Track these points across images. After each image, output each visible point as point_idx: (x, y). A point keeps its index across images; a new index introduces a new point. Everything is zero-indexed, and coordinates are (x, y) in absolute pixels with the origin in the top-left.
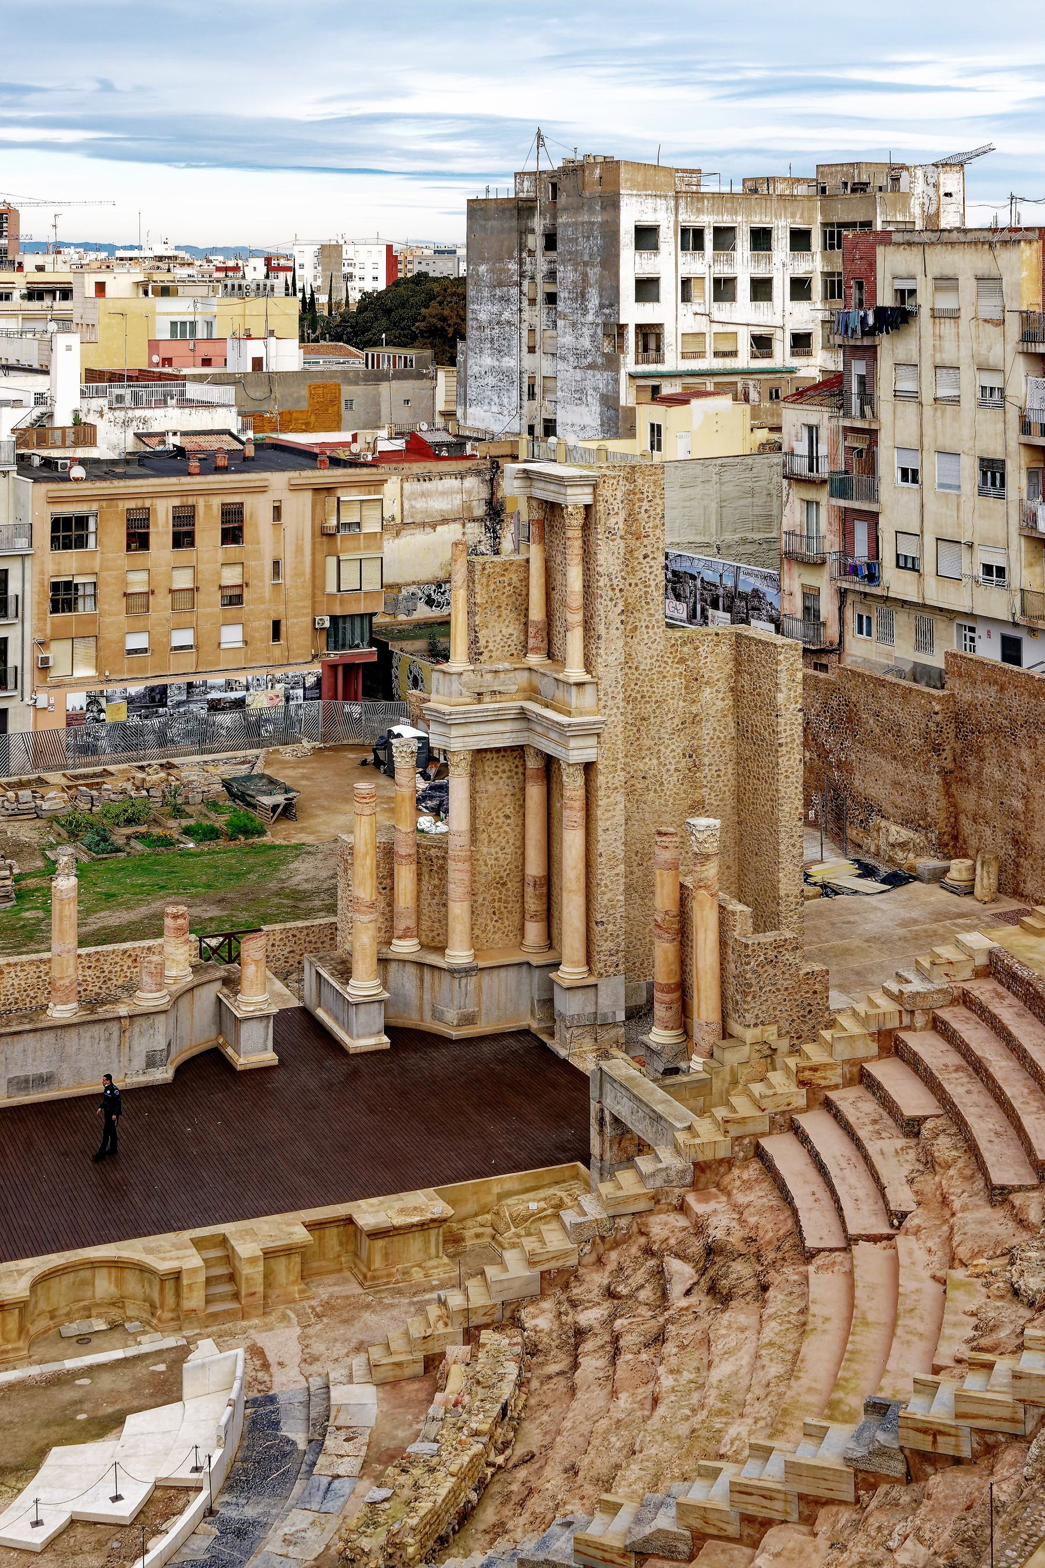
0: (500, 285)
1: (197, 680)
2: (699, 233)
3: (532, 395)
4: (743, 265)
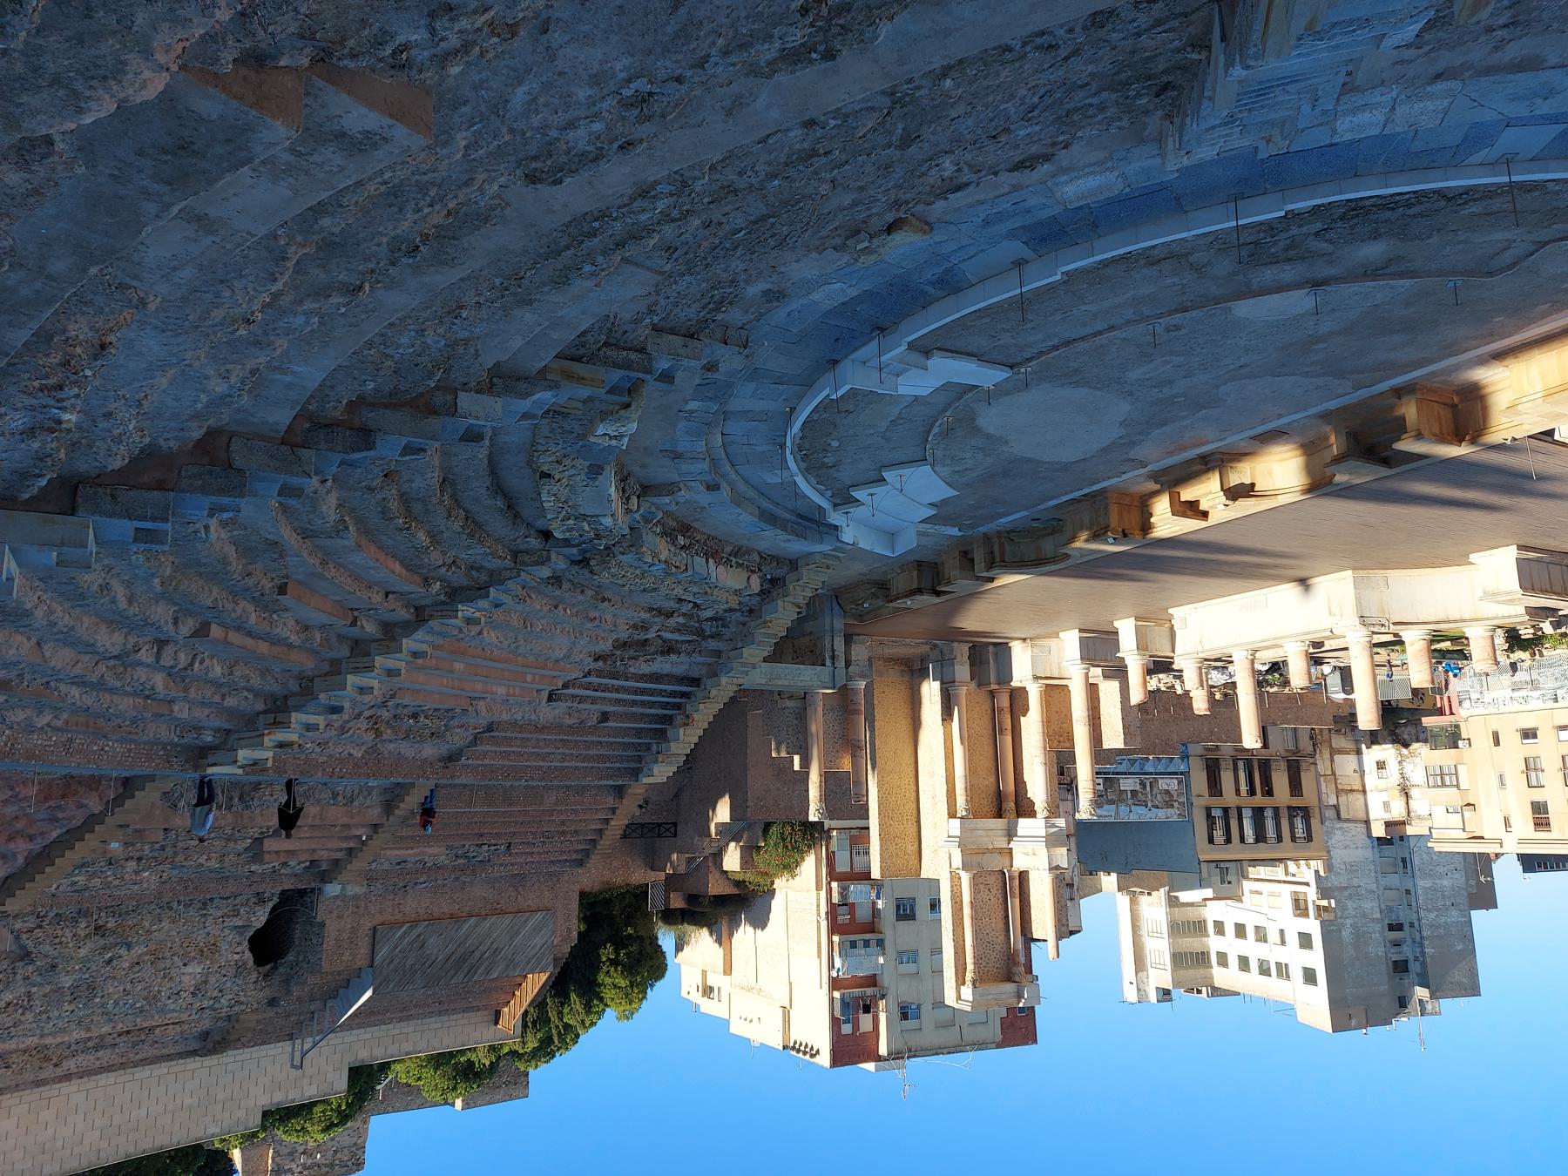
1: (1551, 704)
3: (1404, 860)
4: (1251, 948)
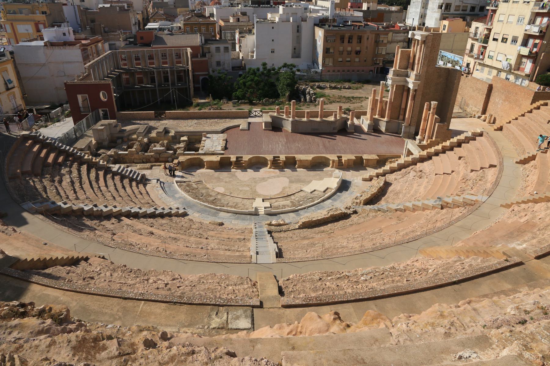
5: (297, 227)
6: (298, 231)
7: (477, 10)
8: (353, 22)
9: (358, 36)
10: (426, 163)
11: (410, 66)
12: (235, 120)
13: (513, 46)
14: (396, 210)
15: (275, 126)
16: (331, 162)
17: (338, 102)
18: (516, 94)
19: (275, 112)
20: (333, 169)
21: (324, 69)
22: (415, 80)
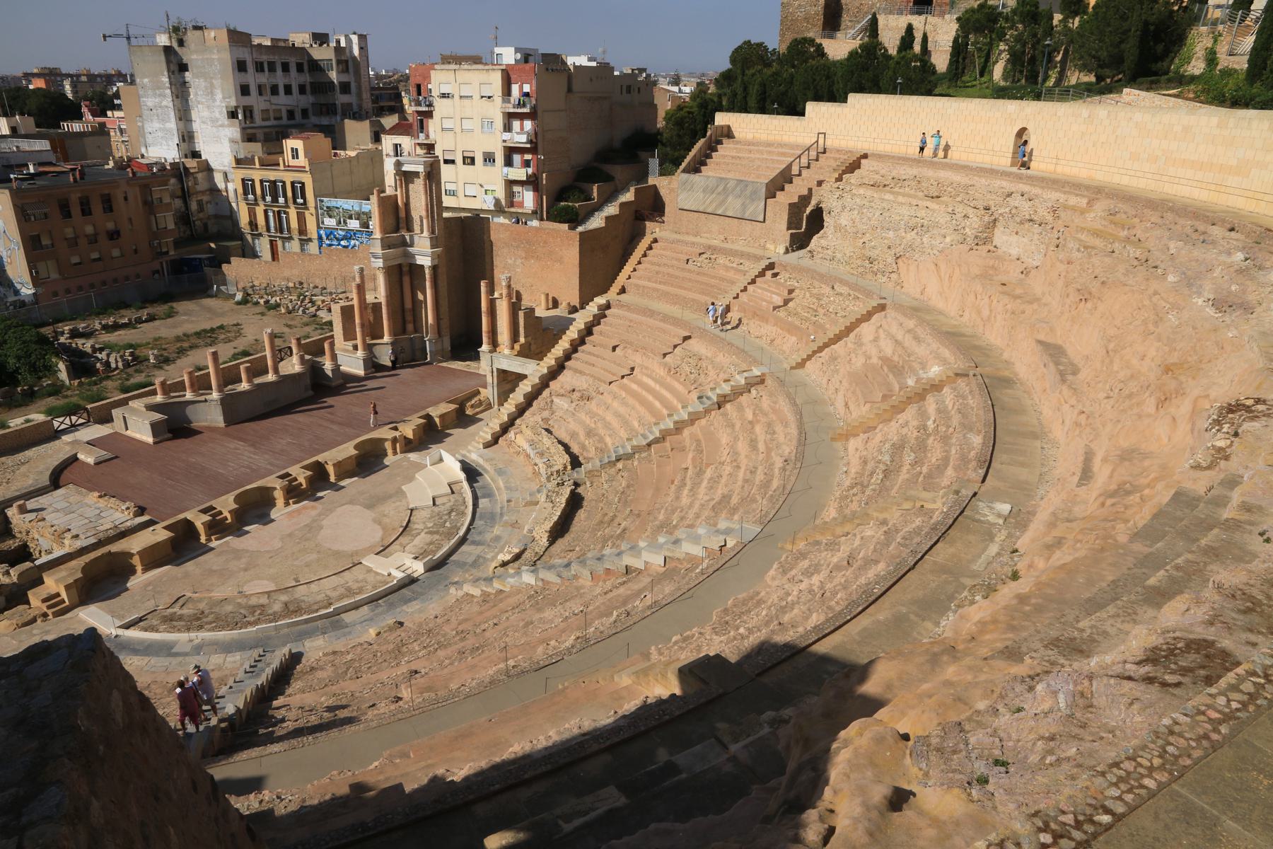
0: (159, 88)
2: (262, 64)
4: (280, 79)
5: (547, 544)
6: (553, 548)
7: (298, 115)
8: (41, 164)
9: (102, 196)
10: (561, 378)
11: (402, 224)
12: (30, 453)
13: (489, 168)
14: (649, 445)
15: (174, 426)
16: (388, 445)
17: (191, 347)
18: (545, 242)
19: (154, 393)
20: (399, 456)
21: (40, 291)
22: (433, 247)
